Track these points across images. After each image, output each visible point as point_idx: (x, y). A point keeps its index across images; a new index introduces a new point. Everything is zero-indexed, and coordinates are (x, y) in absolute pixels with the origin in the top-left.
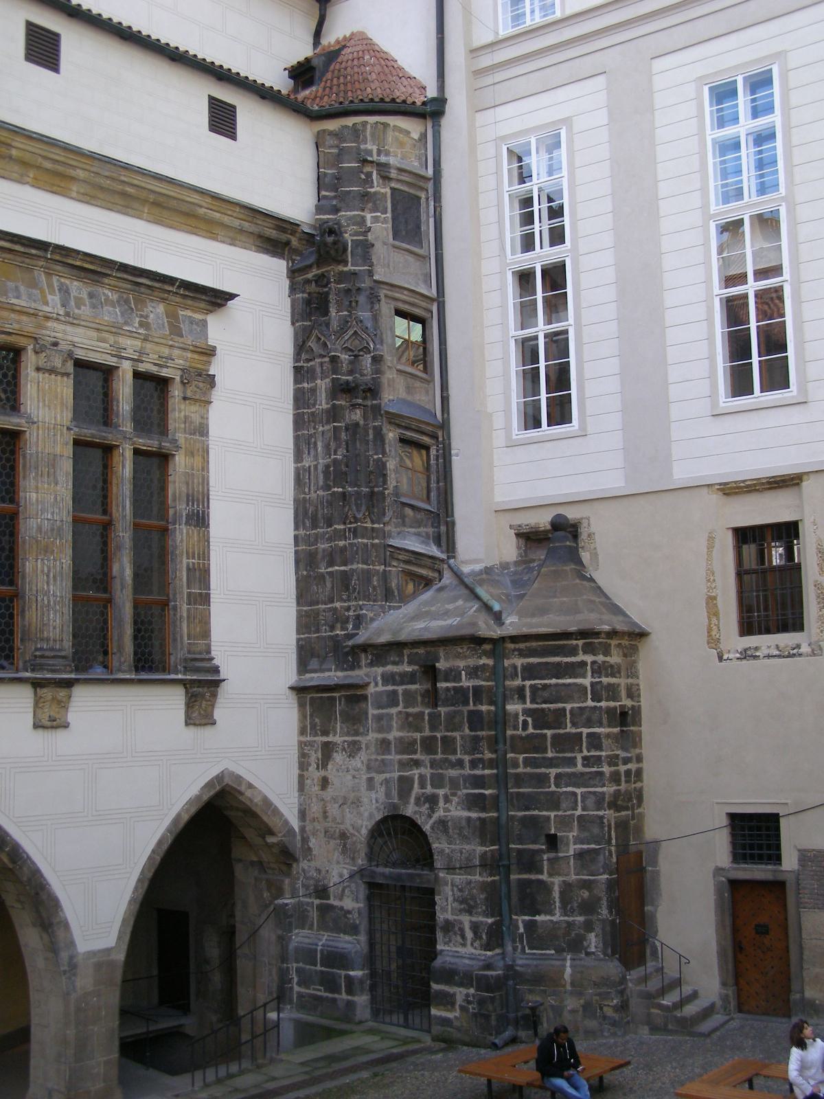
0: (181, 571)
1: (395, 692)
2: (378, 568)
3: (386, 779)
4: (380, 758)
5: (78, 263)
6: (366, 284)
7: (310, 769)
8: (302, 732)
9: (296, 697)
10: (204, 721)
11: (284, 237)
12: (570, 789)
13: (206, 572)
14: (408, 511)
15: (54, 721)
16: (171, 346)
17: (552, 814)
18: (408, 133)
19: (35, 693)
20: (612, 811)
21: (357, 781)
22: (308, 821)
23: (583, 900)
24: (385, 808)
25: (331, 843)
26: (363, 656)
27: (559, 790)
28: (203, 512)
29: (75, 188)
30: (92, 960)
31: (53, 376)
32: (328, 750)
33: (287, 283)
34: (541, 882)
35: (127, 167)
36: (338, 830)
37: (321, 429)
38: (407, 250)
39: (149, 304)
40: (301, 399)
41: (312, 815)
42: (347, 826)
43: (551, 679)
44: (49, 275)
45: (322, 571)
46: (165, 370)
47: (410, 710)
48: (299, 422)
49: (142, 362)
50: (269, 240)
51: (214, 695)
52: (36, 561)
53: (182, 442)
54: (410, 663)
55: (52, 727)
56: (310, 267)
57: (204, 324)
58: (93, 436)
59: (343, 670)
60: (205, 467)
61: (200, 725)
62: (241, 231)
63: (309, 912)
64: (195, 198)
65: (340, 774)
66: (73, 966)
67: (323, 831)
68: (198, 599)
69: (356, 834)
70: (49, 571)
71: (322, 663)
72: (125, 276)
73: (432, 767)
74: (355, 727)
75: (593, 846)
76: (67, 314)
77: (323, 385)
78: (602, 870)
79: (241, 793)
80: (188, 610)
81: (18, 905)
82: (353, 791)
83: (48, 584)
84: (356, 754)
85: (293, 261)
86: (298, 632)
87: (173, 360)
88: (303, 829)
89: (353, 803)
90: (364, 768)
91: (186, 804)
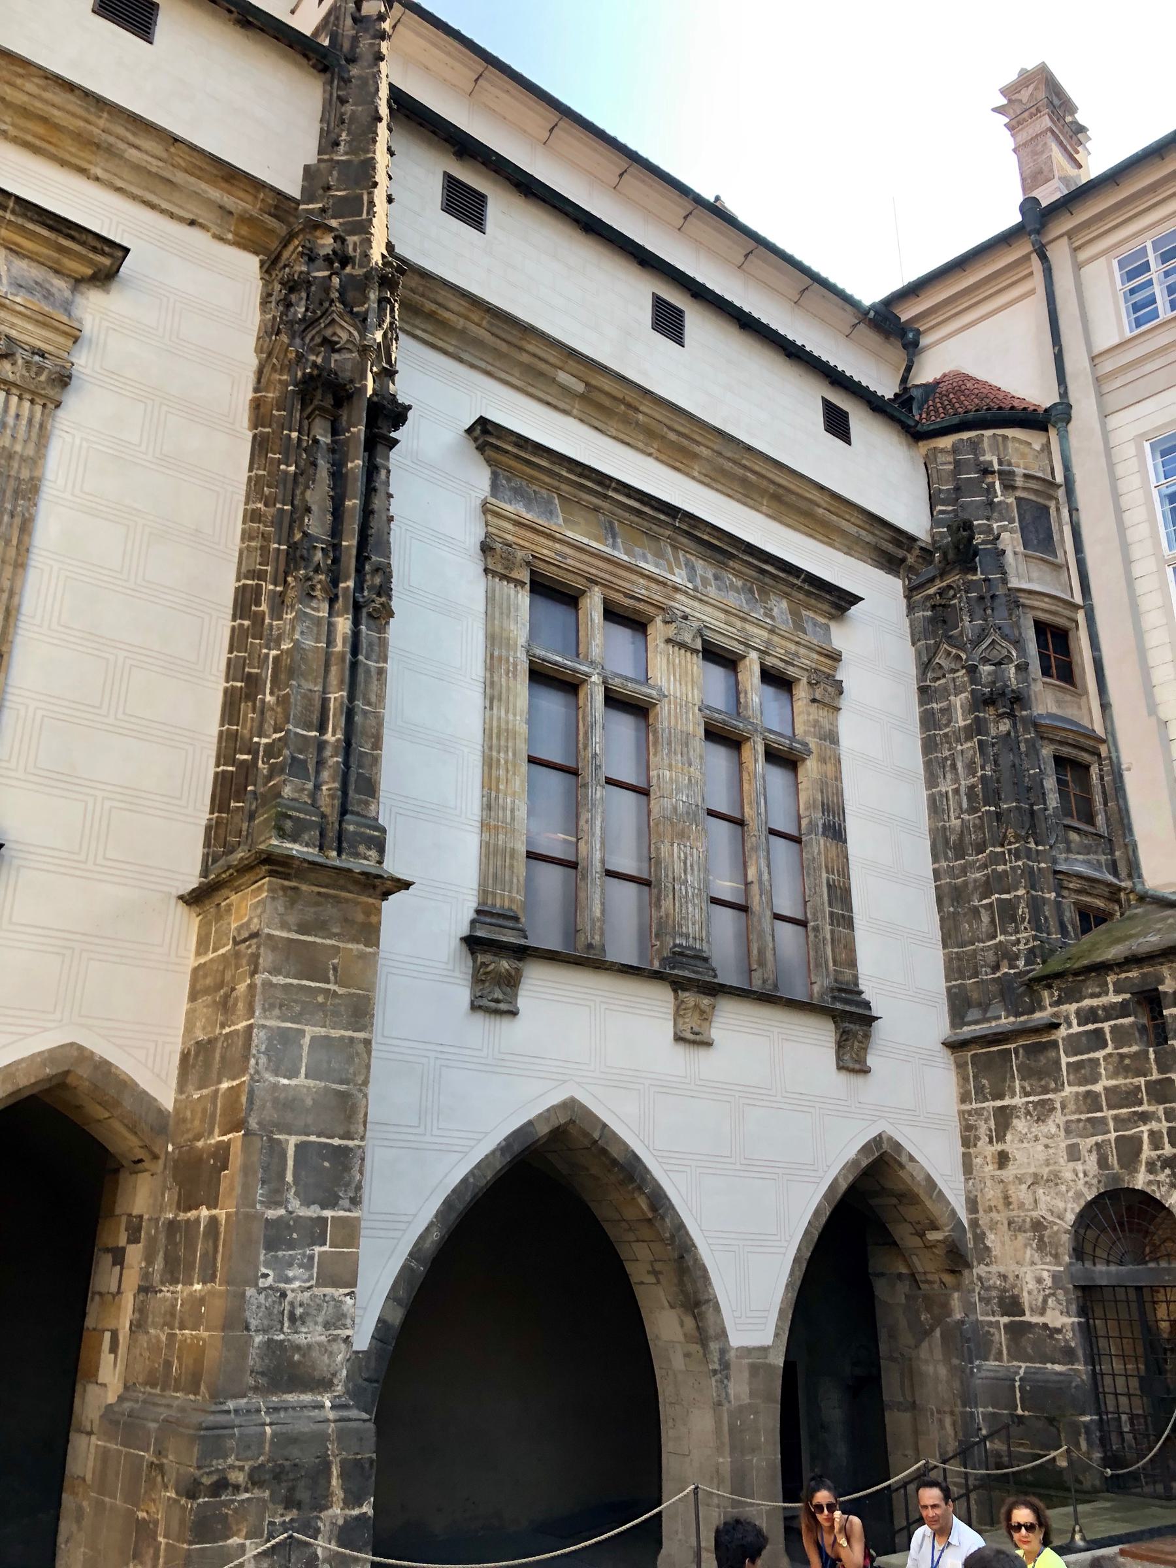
0: (821, 889)
1: (1099, 1033)
2: (1047, 895)
3: (1097, 1144)
4: (1083, 1117)
5: (705, 537)
6: (1000, 591)
7: (979, 1144)
8: (964, 1098)
9: (952, 1058)
11: (900, 553)
13: (847, 892)
14: (1074, 836)
15: (697, 1034)
18: (1030, 444)
19: (676, 998)
21: (1051, 1151)
22: (981, 1211)
24: (1099, 1182)
25: (1020, 1237)
26: (1046, 994)
28: (840, 825)
29: (696, 467)
30: (747, 1361)
31: (683, 651)
32: (1004, 1118)
33: (903, 602)
35: (749, 449)
36: (1028, 1220)
37: (959, 748)
38: (1042, 560)
39: (772, 596)
40: (929, 721)
41: (987, 1204)
42: (1042, 1211)
44: (675, 548)
45: (976, 903)
46: (791, 668)
47: (1125, 1050)
48: (929, 746)
49: (769, 654)
50: (883, 553)
51: (867, 1036)
52: (672, 845)
53: (812, 746)
54: (1117, 992)
55: (694, 1043)
56: (932, 580)
57: (827, 629)
58: (724, 722)
59: (1017, 1015)
60: (838, 778)
62: (858, 540)
63: (993, 1335)
64: (815, 495)
65: (1025, 1145)
66: (726, 1366)
67: (1006, 1223)
69: (1058, 1221)
70: (686, 858)
71: (985, 1011)
72: (751, 560)
73: (1168, 1120)
74: (1043, 1083)
76: (695, 589)
77: (959, 701)
79: (902, 1166)
80: (832, 932)
81: (652, 1279)
82: (1048, 1165)
83: (685, 874)
84: (1048, 1116)
85: (909, 579)
86: (948, 979)
88: (974, 1223)
89: (1048, 1181)
90: (1062, 1133)
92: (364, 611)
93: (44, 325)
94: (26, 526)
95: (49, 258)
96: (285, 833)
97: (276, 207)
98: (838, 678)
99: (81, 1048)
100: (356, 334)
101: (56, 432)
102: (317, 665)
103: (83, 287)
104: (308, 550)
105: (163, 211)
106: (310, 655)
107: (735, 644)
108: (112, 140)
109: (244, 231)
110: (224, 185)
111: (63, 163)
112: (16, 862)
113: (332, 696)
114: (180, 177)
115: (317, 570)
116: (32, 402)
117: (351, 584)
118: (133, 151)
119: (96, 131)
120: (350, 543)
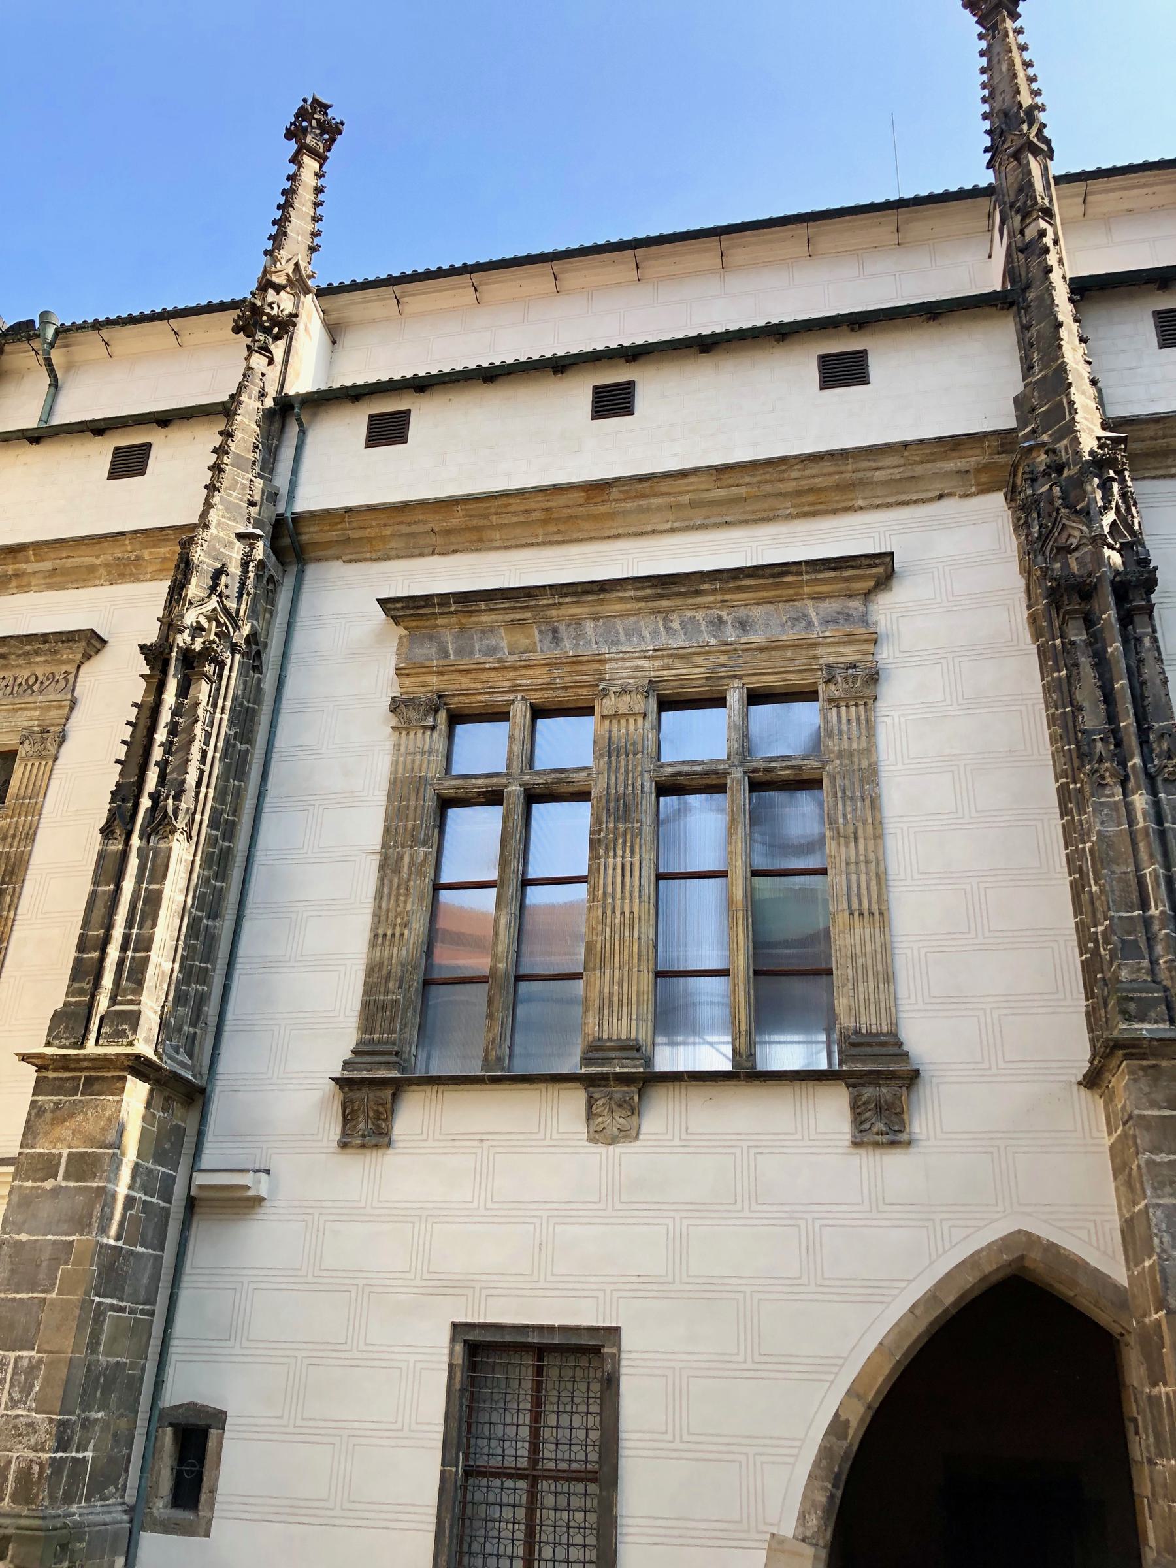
92: (1159, 780)
93: (849, 643)
94: (875, 805)
95: (842, 590)
96: (1130, 1016)
97: (1002, 445)
99: (1028, 1234)
100: (1085, 528)
101: (879, 720)
102: (1125, 847)
103: (872, 597)
104: (1089, 745)
105: (915, 502)
106: (1115, 839)
108: (860, 475)
109: (984, 478)
110: (954, 454)
111: (835, 512)
112: (935, 1080)
113: (1147, 871)
114: (919, 470)
115: (1101, 760)
116: (856, 705)
117: (1137, 760)
118: (878, 473)
119: (848, 475)
120: (1128, 722)
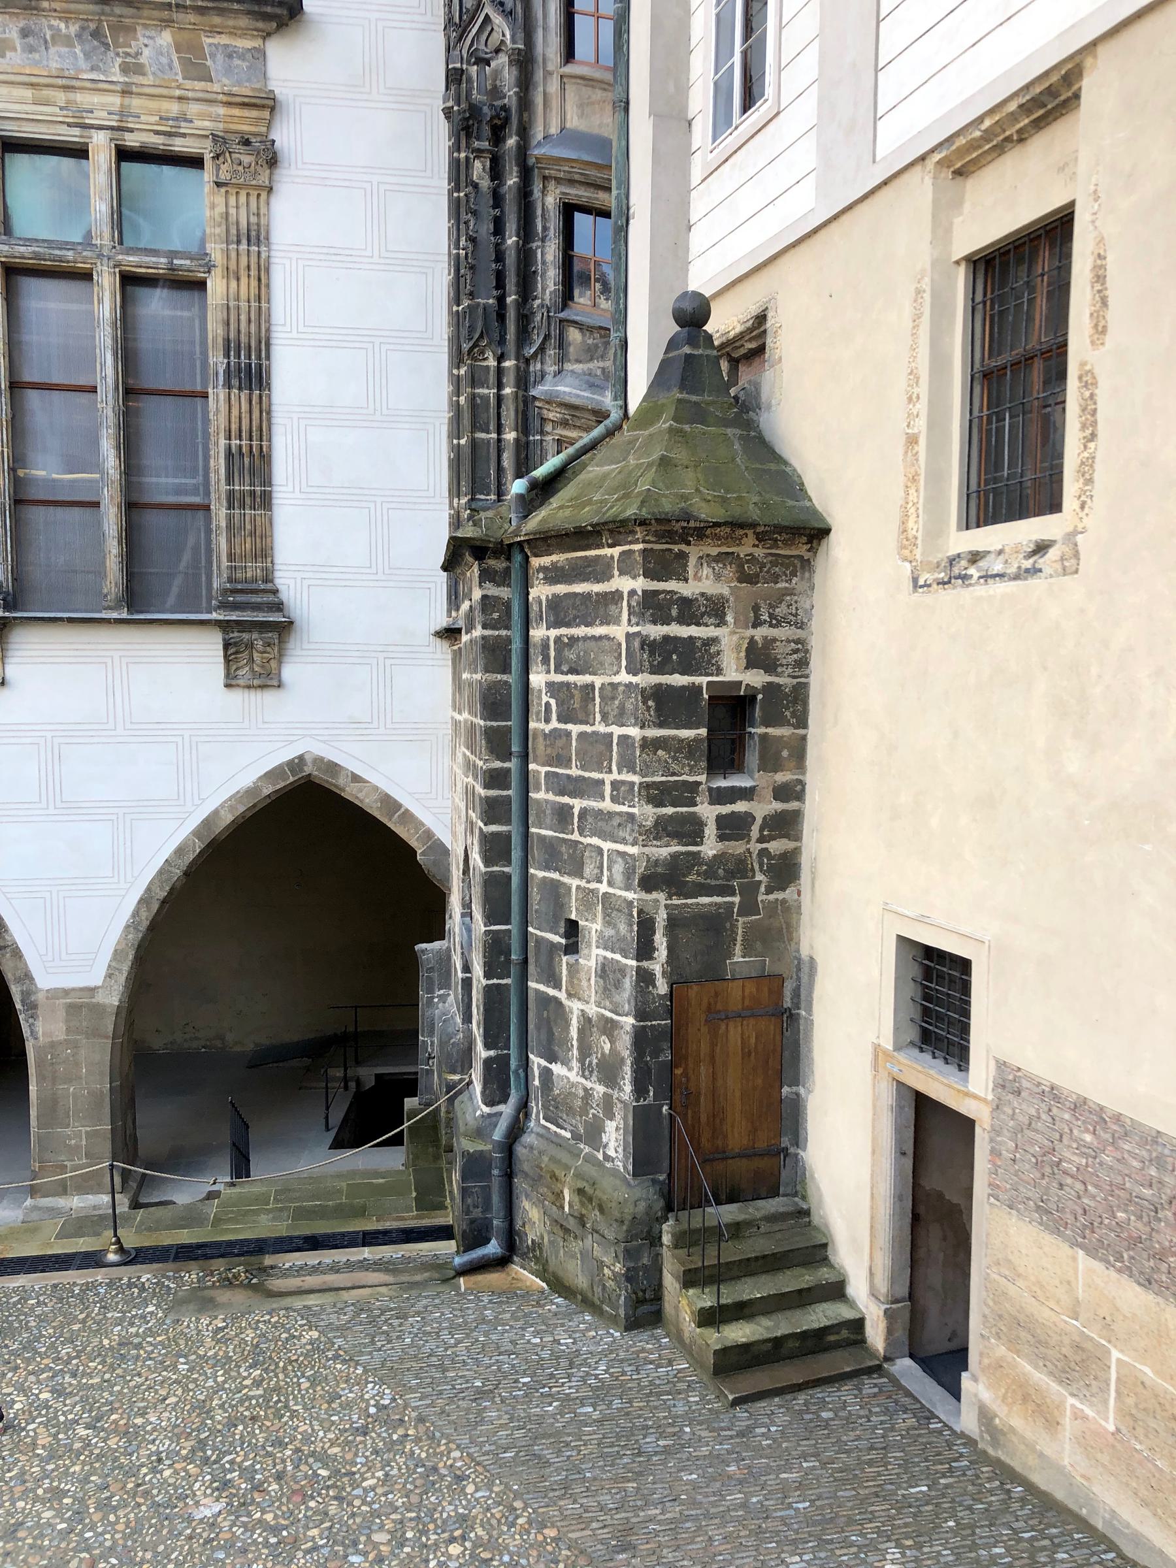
10: (256, 682)
12: (595, 841)
16: (180, 98)
17: (574, 882)
20: (660, 896)
23: (603, 1054)
27: (582, 839)
34: (556, 1000)
43: (578, 625)
49: (131, 130)
57: (260, 55)
61: (249, 687)
68: (248, 500)
75: (618, 957)
78: (627, 1007)
80: (229, 518)
87: (191, 121)
91: (230, 799)
98: (271, 137)
107: (63, 129)
